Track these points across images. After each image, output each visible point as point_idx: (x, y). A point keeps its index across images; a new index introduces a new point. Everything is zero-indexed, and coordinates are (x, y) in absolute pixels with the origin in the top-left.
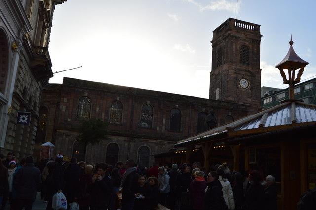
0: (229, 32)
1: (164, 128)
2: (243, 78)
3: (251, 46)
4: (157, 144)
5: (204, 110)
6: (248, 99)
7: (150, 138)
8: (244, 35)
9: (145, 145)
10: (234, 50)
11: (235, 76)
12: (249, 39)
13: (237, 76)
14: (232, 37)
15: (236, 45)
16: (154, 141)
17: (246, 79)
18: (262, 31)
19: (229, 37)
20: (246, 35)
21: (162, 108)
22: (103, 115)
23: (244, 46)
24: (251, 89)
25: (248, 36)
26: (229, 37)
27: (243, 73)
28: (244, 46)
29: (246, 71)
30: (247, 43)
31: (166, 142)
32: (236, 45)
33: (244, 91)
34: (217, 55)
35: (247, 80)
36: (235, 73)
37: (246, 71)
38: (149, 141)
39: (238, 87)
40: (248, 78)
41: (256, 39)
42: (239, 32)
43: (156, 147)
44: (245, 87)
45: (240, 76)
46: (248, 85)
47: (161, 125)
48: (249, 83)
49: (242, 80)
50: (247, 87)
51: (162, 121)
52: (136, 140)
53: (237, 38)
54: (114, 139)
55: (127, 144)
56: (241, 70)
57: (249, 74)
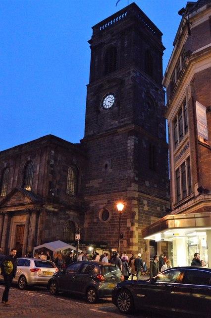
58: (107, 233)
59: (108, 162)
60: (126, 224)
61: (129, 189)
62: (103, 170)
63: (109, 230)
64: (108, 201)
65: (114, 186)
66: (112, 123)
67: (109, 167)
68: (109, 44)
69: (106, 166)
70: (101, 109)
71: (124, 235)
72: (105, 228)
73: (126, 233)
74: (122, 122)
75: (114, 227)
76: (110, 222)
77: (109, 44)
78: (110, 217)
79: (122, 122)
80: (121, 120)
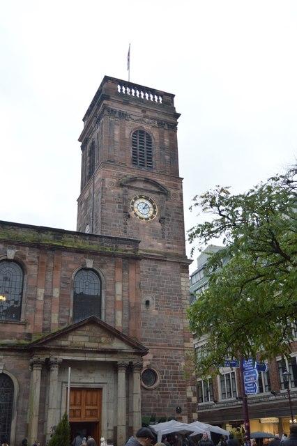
0: (105, 102)
2: (141, 197)
3: (155, 134)
5: (11, 254)
6: (154, 242)
8: (140, 111)
10: (117, 139)
11: (120, 191)
12: (151, 119)
13: (126, 191)
14: (112, 112)
15: (122, 130)
17: (146, 198)
18: (179, 105)
19: (106, 112)
20: (144, 111)
23: (140, 133)
24: (161, 220)
25: (148, 113)
26: (106, 112)
27: (141, 185)
28: (140, 133)
29: (147, 181)
30: (147, 128)
32: (122, 130)
33: (144, 225)
34: (88, 158)
35: (151, 202)
36: (122, 185)
37: (147, 181)
39: (129, 216)
40: (152, 196)
41: (168, 119)
42: (126, 103)
44: (146, 216)
45: (132, 193)
46: (154, 213)
48: (154, 207)
49: (135, 205)
50: (152, 217)
53: (123, 115)
56: (134, 180)
57: (154, 188)
58: (155, 405)
59: (150, 299)
60: (186, 394)
61: (187, 345)
62: (143, 307)
63: (159, 400)
64: (154, 357)
65: (163, 336)
66: (152, 243)
67: (152, 307)
68: (139, 125)
69: (147, 303)
70: (132, 213)
71: (183, 408)
72: (151, 397)
73: (185, 405)
74: (169, 248)
75: (168, 397)
76: (159, 389)
77: (139, 125)
78: (158, 381)
79: (169, 248)
80: (167, 245)
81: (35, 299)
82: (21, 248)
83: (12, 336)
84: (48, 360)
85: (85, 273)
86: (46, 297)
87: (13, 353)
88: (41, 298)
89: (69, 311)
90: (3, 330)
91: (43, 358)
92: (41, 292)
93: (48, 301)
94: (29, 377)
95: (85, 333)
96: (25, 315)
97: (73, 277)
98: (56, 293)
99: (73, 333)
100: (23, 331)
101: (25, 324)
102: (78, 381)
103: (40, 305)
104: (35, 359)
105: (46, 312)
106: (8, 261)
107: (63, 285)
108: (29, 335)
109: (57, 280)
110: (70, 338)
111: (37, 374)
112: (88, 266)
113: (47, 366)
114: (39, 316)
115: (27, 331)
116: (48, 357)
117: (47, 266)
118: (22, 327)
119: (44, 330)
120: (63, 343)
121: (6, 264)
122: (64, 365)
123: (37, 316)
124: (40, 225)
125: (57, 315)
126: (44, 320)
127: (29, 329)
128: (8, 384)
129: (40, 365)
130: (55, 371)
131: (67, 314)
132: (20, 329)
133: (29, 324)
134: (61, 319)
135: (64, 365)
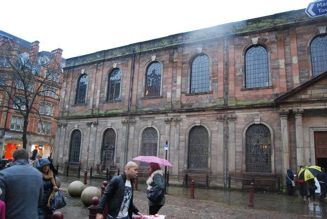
1: (178, 91)
4: (167, 122)
5: (255, 40)
7: (158, 113)
9: (149, 125)
16: (163, 117)
21: (174, 61)
22: (99, 91)
31: (183, 116)
38: (156, 118)
43: (167, 127)
47: (174, 88)
51: (176, 82)
52: (137, 119)
54: (110, 123)
55: (125, 128)
81: (278, 68)
82: (262, 34)
83: (264, 96)
84: (291, 111)
85: (319, 39)
86: (286, 65)
87: (266, 109)
88: (283, 66)
89: (308, 72)
90: (257, 94)
91: (287, 110)
92: (282, 62)
93: (288, 68)
94: (280, 125)
95: (322, 86)
96: (272, 81)
97: (308, 45)
98: (295, 60)
99: (311, 88)
100: (272, 93)
101: (273, 87)
102: (324, 126)
103: (282, 72)
104: (280, 111)
105: (288, 76)
106: (253, 46)
107: (300, 53)
108: (277, 95)
109: (294, 51)
110: (309, 92)
111: (284, 122)
112: (321, 33)
113: (291, 116)
114: (283, 80)
115: (275, 93)
116: (291, 108)
117: (284, 42)
118: (272, 90)
119: (288, 89)
120: (303, 97)
121: (253, 49)
122: (306, 114)
123: (281, 80)
124: (274, 14)
125: (298, 76)
126: (287, 82)
127: (277, 91)
128: (266, 131)
129: (286, 115)
130: (299, 119)
131: (306, 74)
132: (270, 92)
133: (276, 87)
134: (302, 79)
135: (306, 114)
